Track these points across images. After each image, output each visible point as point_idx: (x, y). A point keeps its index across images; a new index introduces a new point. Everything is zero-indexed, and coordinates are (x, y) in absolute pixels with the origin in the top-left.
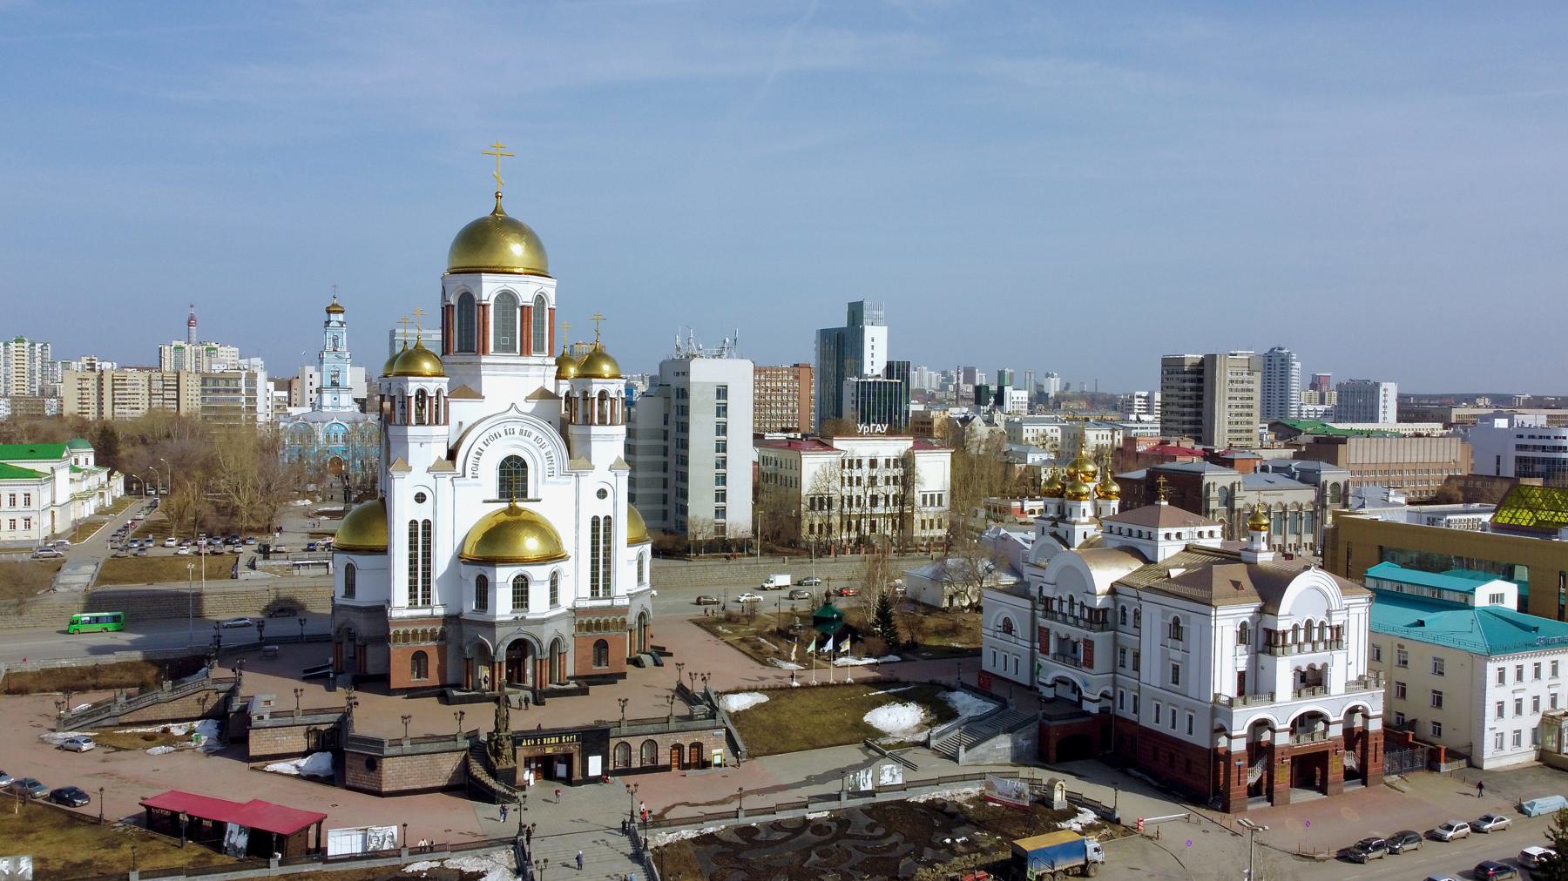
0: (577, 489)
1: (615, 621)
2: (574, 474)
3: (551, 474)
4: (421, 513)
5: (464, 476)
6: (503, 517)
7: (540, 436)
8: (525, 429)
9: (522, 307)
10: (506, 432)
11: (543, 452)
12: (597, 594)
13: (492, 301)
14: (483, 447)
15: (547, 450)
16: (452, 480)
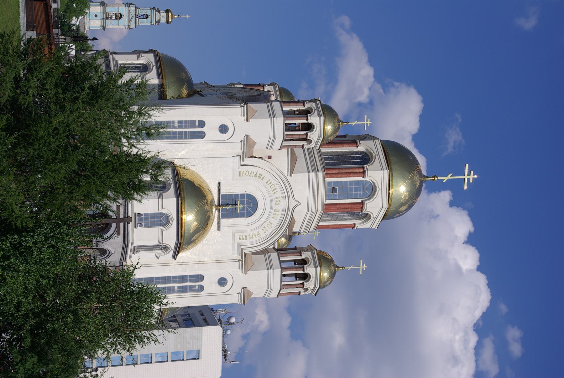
0: (228, 261)
2: (240, 258)
3: (241, 238)
4: (211, 131)
5: (242, 165)
6: (209, 198)
7: (273, 227)
9: (362, 203)
11: (260, 231)
13: (367, 179)
14: (265, 180)
16: (238, 156)
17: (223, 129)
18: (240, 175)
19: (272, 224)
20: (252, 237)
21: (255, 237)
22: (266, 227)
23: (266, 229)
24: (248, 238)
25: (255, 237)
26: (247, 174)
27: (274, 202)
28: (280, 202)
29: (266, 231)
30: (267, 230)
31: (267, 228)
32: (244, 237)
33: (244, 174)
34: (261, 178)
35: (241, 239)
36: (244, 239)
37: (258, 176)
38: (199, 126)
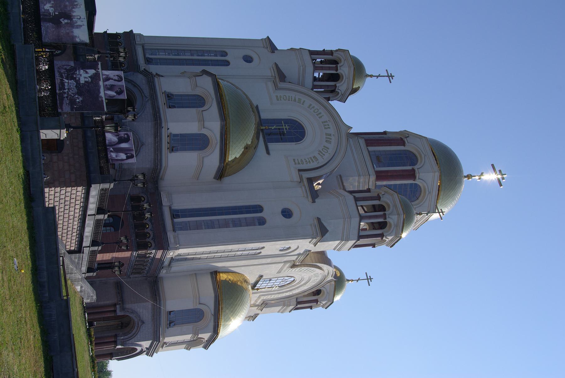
1: (145, 235)
3: (297, 161)
8: (332, 137)
10: (325, 122)
12: (178, 216)
13: (407, 148)
15: (318, 157)
17: (248, 59)
19: (327, 148)
20: (309, 162)
22: (322, 151)
23: (322, 153)
24: (305, 163)
26: (285, 99)
28: (329, 126)
29: (323, 155)
30: (324, 155)
31: (325, 153)
32: (300, 162)
33: (282, 99)
38: (222, 56)
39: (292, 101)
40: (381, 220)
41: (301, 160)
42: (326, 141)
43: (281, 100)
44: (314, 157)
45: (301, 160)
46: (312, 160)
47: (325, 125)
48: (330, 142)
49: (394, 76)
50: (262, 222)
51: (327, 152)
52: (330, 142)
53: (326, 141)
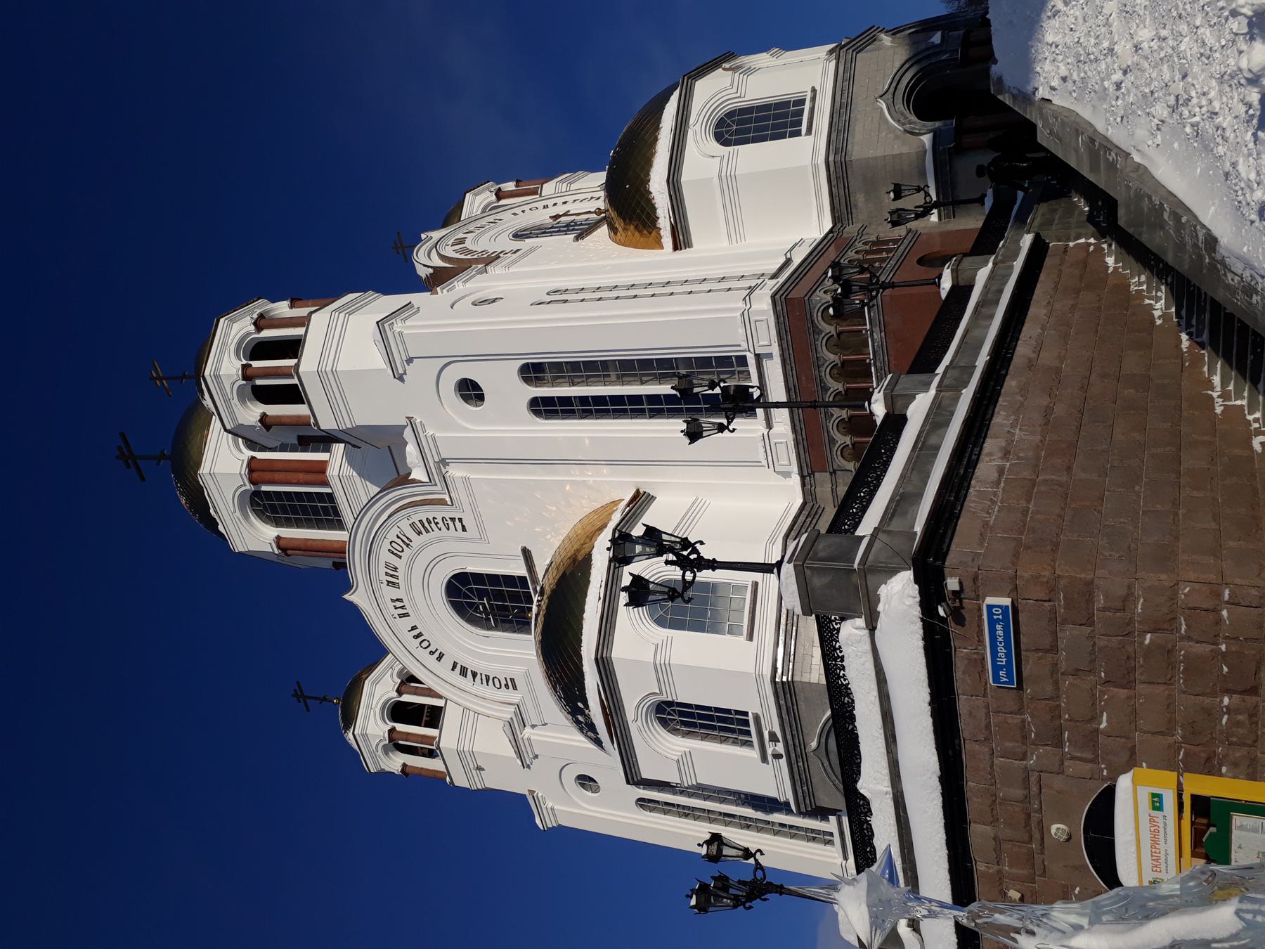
3: (458, 525)
8: (385, 578)
14: (447, 662)
18: (512, 680)
19: (392, 553)
21: (421, 521)
22: (404, 546)
25: (421, 521)
26: (495, 680)
27: (406, 603)
28: (394, 604)
29: (400, 535)
30: (398, 537)
32: (451, 524)
33: (503, 682)
34: (458, 667)
35: (457, 520)
36: (449, 520)
37: (469, 674)
39: (481, 674)
40: (256, 364)
41: (448, 529)
42: (396, 569)
43: (506, 678)
44: (419, 533)
45: (448, 529)
46: (423, 526)
47: (402, 607)
48: (387, 565)
49: (293, 696)
50: (533, 372)
51: (391, 543)
52: (387, 565)
53: (396, 569)
